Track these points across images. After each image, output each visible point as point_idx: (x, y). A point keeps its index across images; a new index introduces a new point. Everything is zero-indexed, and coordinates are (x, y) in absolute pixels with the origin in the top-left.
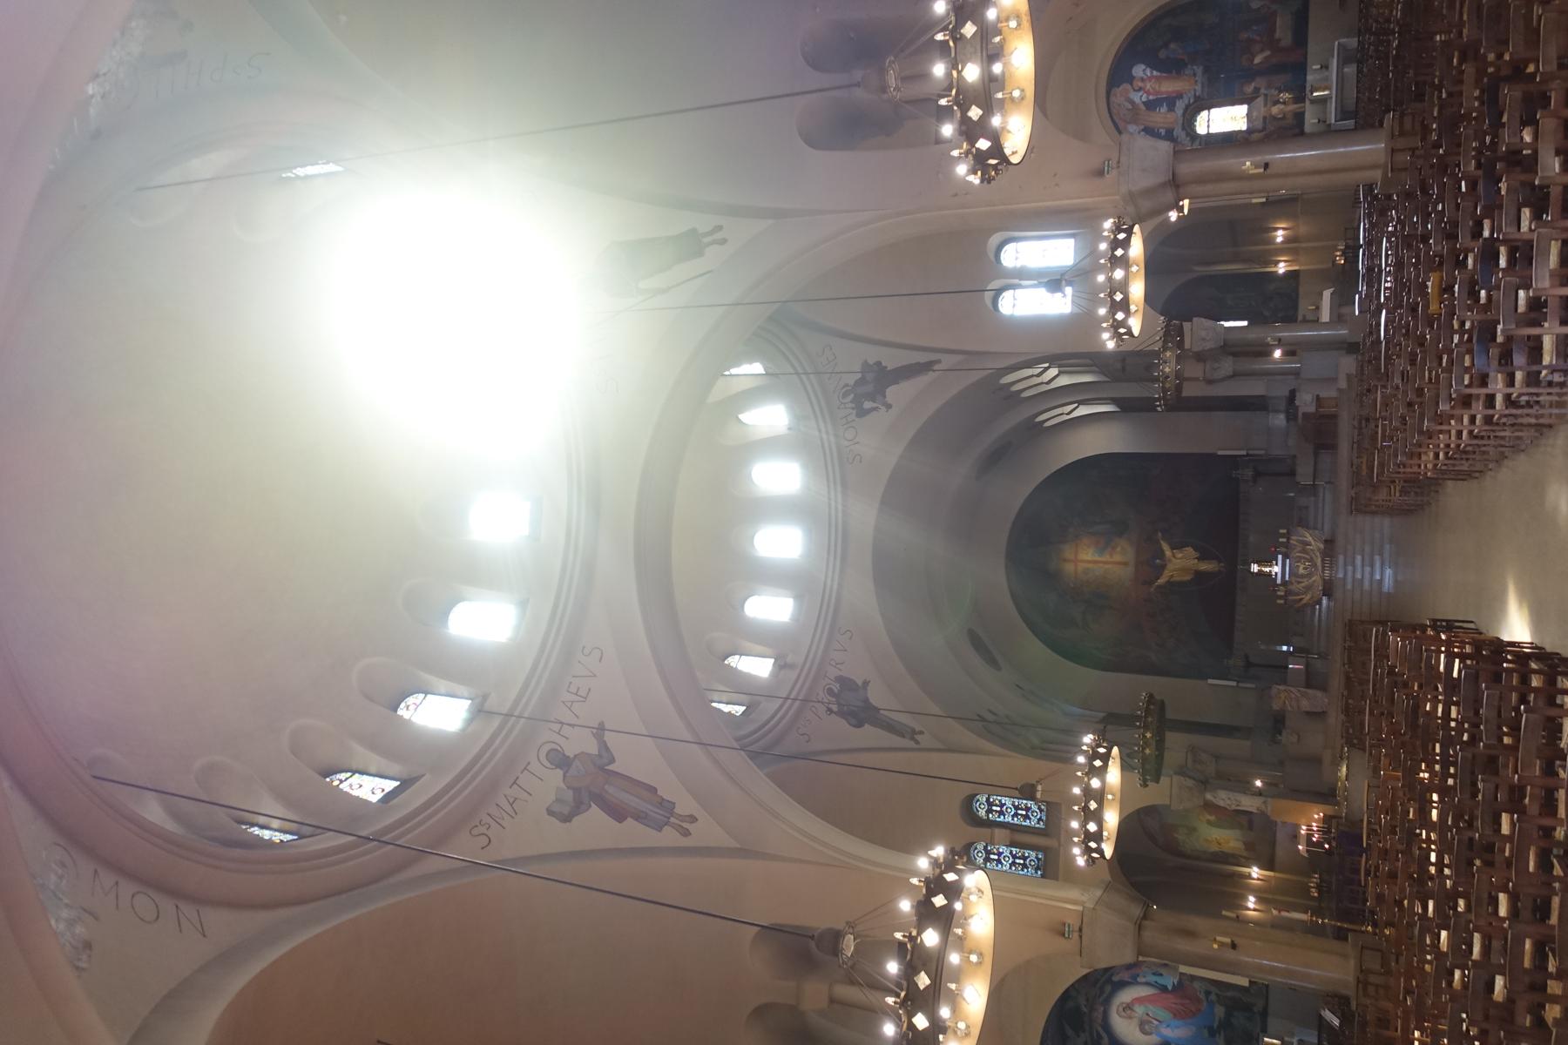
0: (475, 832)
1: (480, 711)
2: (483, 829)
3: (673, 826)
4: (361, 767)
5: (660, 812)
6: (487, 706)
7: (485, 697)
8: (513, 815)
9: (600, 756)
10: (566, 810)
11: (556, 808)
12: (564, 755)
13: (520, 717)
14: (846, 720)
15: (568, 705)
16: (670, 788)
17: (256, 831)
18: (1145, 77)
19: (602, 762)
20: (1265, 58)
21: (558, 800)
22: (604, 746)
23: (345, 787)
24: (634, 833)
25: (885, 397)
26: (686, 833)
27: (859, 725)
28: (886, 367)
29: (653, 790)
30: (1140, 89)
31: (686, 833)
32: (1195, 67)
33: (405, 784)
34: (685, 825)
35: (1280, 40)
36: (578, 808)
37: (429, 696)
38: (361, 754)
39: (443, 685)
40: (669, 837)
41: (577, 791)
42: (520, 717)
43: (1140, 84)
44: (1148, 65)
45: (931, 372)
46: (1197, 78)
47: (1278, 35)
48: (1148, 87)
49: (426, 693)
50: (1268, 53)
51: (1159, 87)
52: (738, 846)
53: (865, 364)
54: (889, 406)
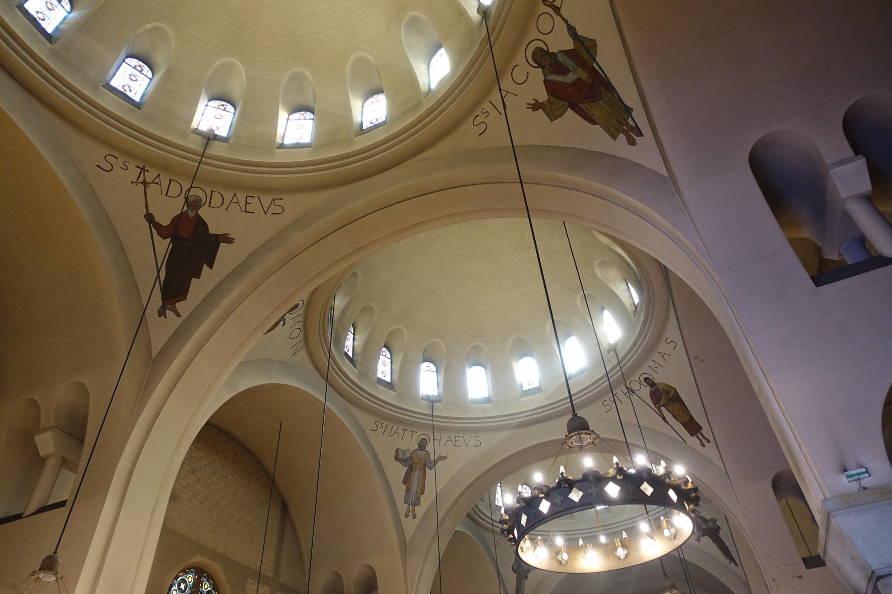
0: (377, 423)
1: (432, 402)
2: (379, 425)
3: (409, 507)
4: (394, 361)
5: (413, 501)
6: (436, 405)
7: (440, 401)
8: (391, 435)
9: (431, 462)
10: (401, 457)
11: (400, 452)
12: (426, 445)
13: (433, 421)
14: (515, 563)
15: (449, 439)
16: (427, 500)
17: (351, 336)
19: (428, 464)
21: (404, 452)
22: (436, 462)
23: (382, 358)
24: (400, 490)
25: (703, 536)
26: (407, 516)
27: (514, 571)
28: (719, 533)
29: (423, 493)
31: (407, 516)
33: (389, 385)
34: (411, 514)
36: (403, 461)
37: (436, 373)
38: (398, 359)
39: (441, 379)
40: (402, 508)
41: (411, 458)
42: (433, 421)
45: (729, 561)
49: (437, 372)
52: (407, 543)
53: (714, 521)
54: (698, 540)
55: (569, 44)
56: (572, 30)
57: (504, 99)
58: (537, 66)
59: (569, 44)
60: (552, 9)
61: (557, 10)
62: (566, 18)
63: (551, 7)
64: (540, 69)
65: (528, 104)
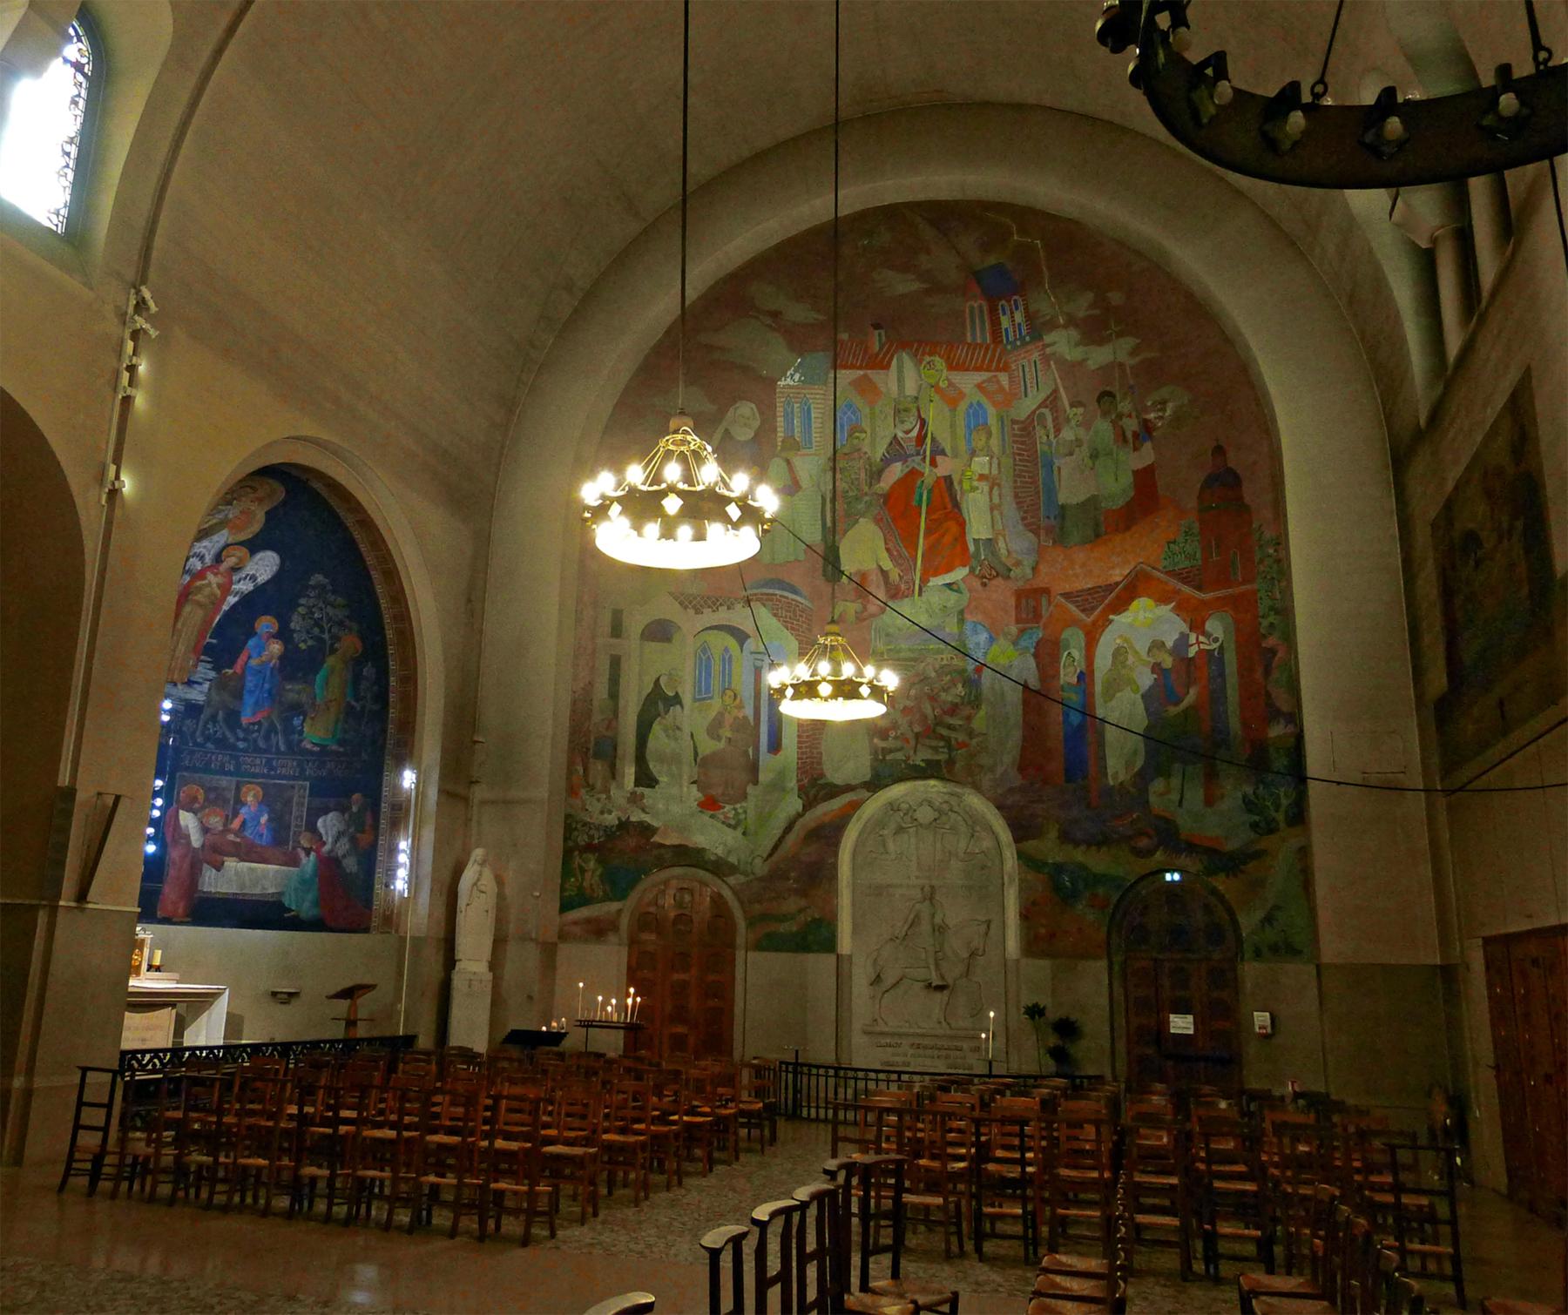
18: (235, 578)
20: (188, 837)
30: (218, 559)
32: (207, 685)
35: (219, 867)
43: (230, 561)
44: (260, 590)
46: (180, 687)
47: (231, 864)
48: (210, 577)
50: (196, 840)
51: (200, 604)
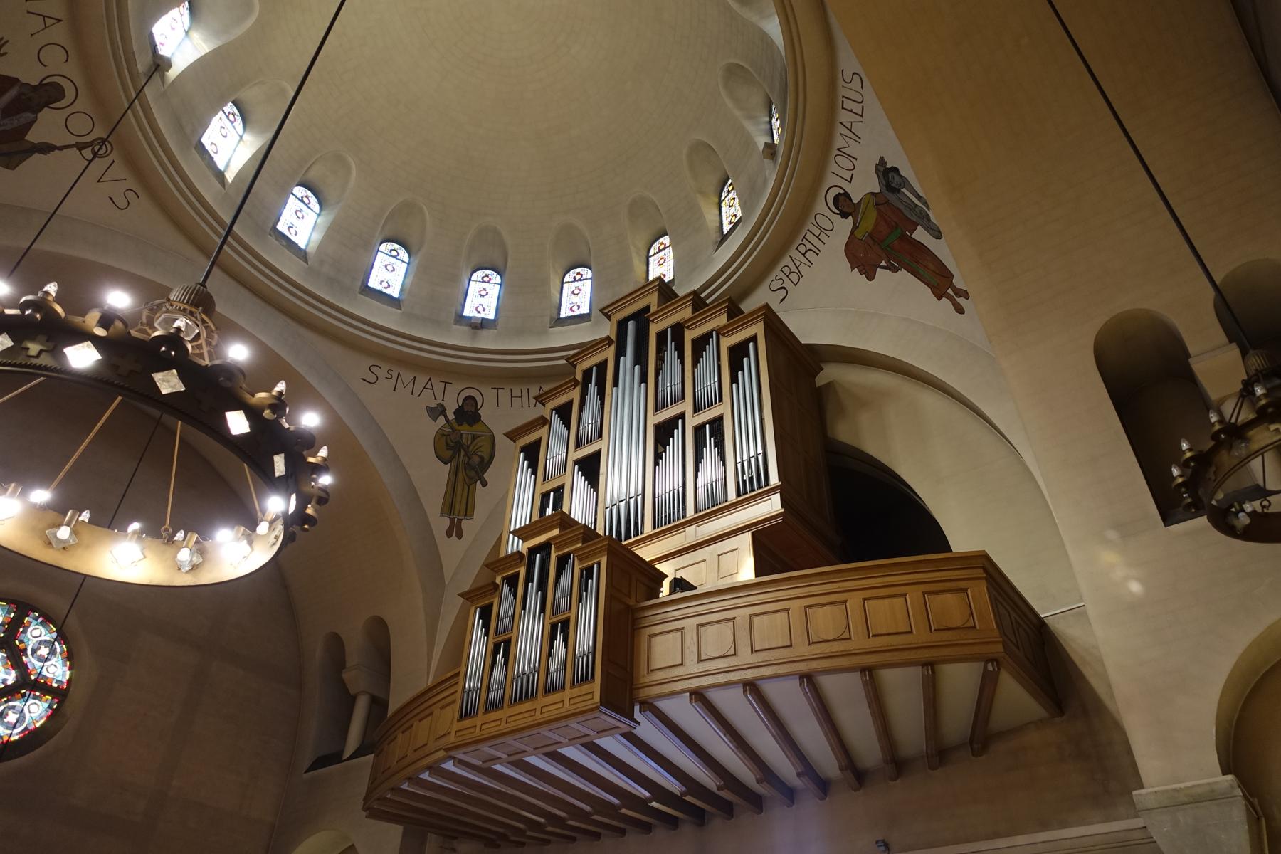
55: (33, 136)
56: (46, 148)
57: (42, 17)
58: (44, 82)
59: (33, 136)
60: (87, 143)
61: (81, 147)
62: (65, 150)
63: (90, 142)
64: (37, 83)
65: (7, 42)
